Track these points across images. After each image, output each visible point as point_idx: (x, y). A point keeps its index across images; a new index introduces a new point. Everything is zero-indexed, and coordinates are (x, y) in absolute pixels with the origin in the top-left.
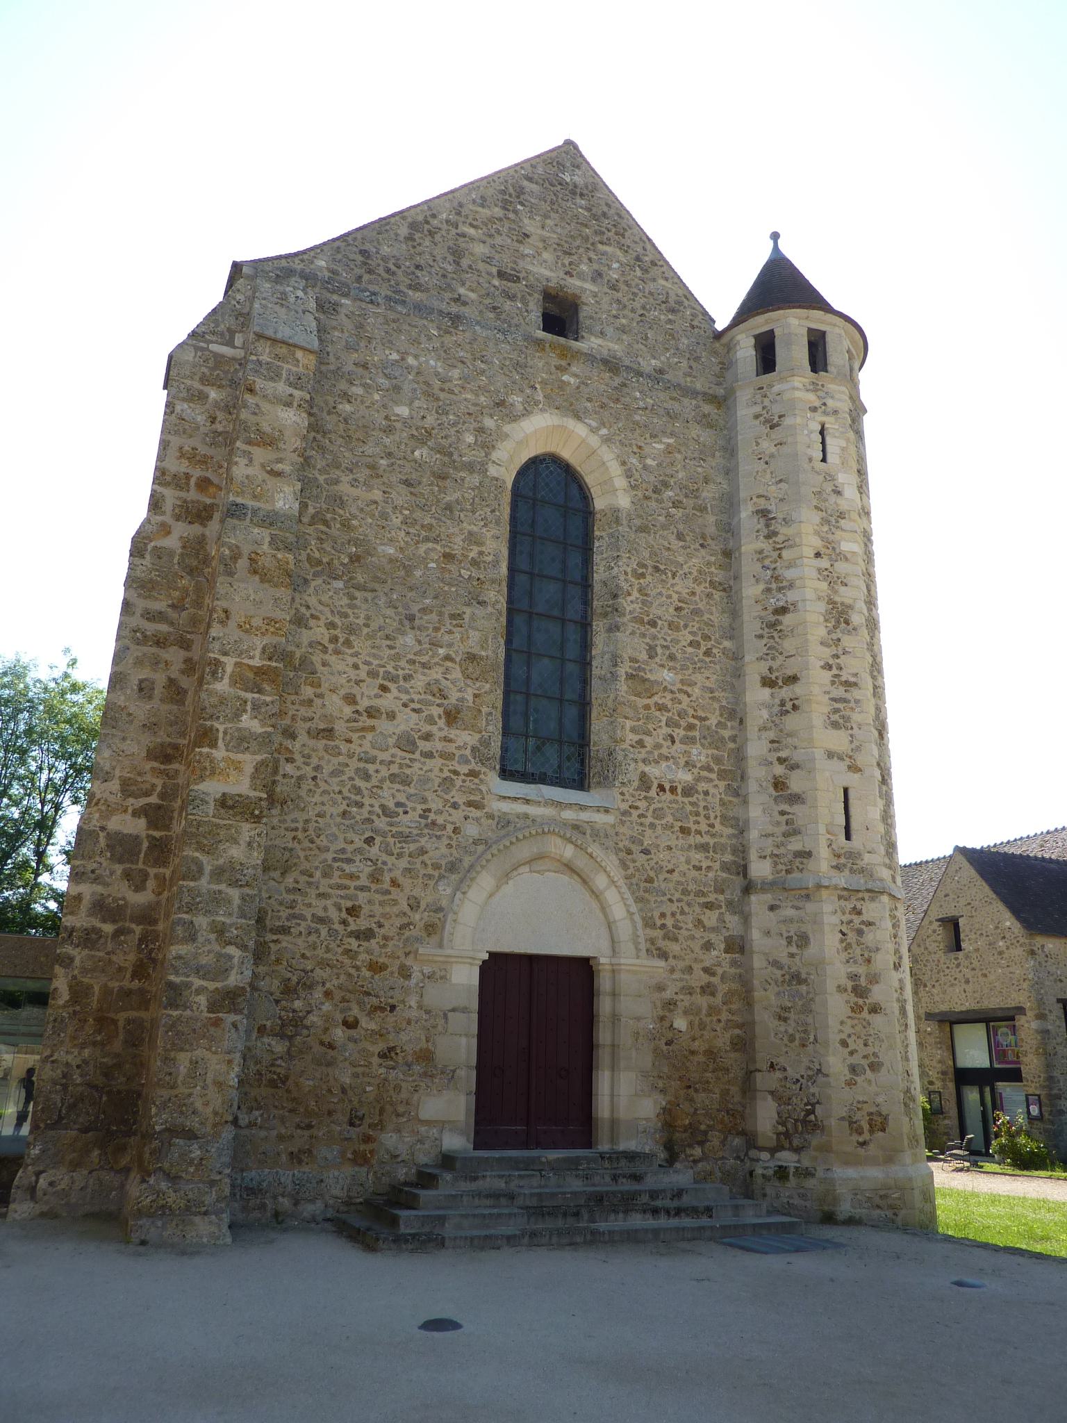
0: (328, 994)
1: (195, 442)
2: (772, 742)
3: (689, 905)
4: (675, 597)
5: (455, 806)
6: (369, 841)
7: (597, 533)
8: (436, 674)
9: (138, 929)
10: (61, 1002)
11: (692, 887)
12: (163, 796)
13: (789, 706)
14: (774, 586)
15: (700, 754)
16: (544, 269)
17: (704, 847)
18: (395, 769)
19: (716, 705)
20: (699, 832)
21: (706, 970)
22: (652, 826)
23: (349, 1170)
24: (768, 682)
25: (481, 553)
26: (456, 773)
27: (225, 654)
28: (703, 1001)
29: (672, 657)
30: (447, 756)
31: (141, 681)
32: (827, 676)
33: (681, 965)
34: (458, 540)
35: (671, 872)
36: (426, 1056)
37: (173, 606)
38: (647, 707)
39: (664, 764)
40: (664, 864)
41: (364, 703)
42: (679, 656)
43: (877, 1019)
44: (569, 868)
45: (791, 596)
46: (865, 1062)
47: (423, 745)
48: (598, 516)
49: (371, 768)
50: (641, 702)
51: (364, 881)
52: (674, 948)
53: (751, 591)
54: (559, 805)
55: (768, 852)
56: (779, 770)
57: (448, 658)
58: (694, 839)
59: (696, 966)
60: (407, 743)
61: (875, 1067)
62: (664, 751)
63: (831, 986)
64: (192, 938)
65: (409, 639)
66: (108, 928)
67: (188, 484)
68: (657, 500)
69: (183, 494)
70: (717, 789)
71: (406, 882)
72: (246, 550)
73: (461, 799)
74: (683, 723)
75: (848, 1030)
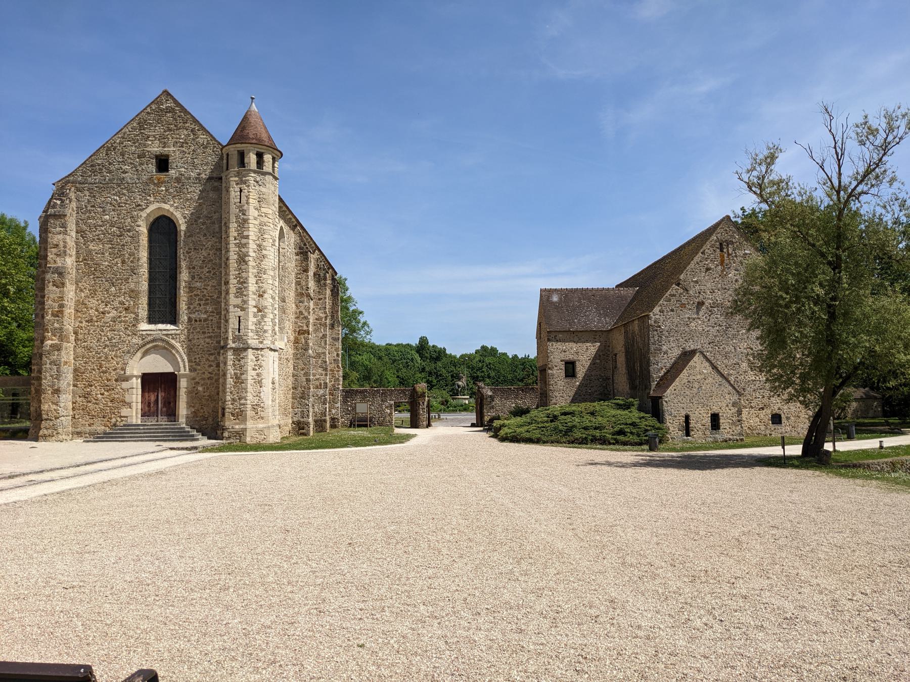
8: (122, 298)
15: (209, 308)
16: (155, 148)
17: (210, 337)
28: (209, 382)
29: (200, 278)
32: (235, 281)
34: (127, 255)
60: (114, 320)
63: (229, 376)
65: (113, 289)
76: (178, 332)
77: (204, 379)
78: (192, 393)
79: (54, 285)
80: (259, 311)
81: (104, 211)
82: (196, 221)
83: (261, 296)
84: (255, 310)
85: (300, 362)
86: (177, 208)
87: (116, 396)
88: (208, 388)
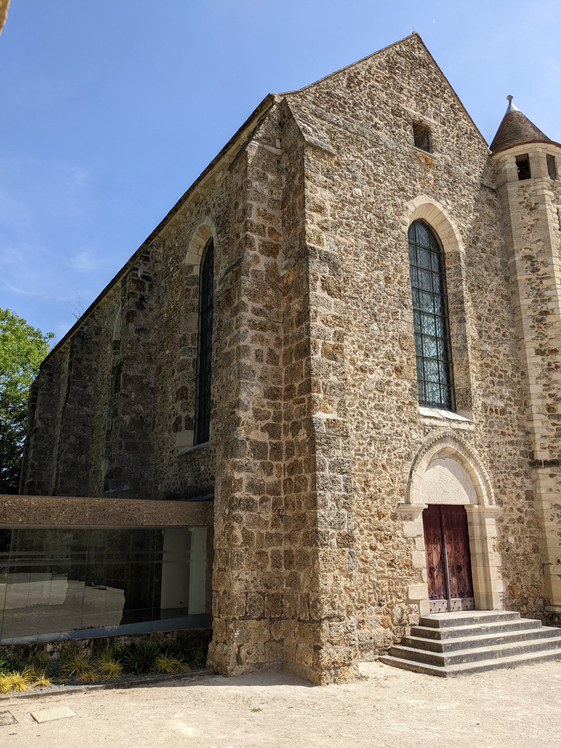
0: (361, 531)
1: (265, 205)
2: (544, 385)
3: (509, 474)
4: (487, 303)
5: (405, 422)
6: (370, 444)
7: (447, 266)
9: (271, 498)
10: (239, 544)
12: (275, 419)
13: (553, 366)
14: (539, 299)
15: (506, 392)
17: (511, 443)
19: (510, 364)
20: (509, 435)
23: (382, 629)
24: (539, 352)
25: (401, 277)
27: (318, 337)
29: (489, 337)
31: (256, 351)
33: (508, 507)
35: (500, 457)
37: (266, 306)
39: (491, 397)
40: (497, 452)
42: (492, 337)
44: (455, 456)
45: (550, 305)
48: (447, 256)
51: (369, 467)
53: (525, 302)
54: (449, 420)
55: (547, 445)
56: (550, 401)
57: (393, 337)
59: (515, 508)
60: (381, 387)
62: (490, 390)
64: (326, 504)
66: (257, 498)
67: (264, 232)
68: (475, 248)
69: (263, 238)
70: (514, 409)
72: (320, 276)
73: (407, 420)
76: (472, 427)
78: (504, 548)
79: (324, 288)
87: (397, 553)
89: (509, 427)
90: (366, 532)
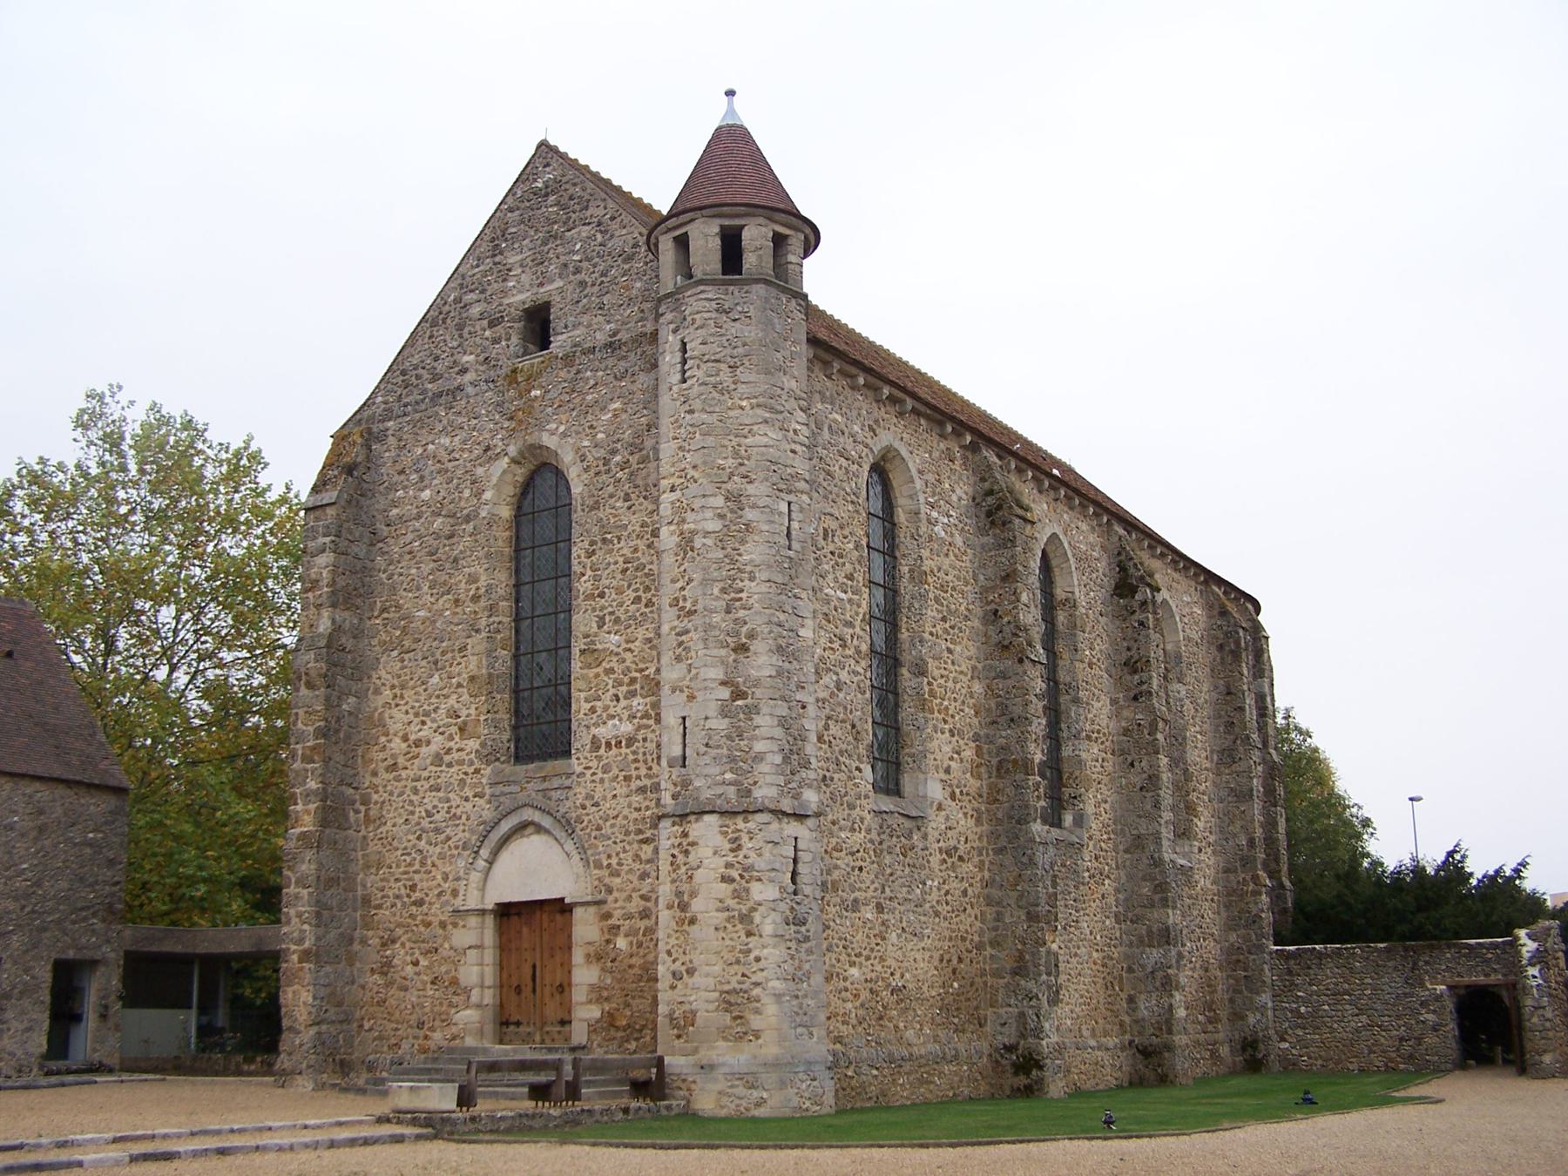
0: (403, 945)
4: (621, 560)
5: (467, 799)
6: (419, 838)
8: (452, 701)
11: (632, 828)
15: (638, 703)
16: (520, 296)
18: (432, 782)
20: (639, 777)
21: (642, 897)
22: (602, 780)
26: (466, 774)
29: (617, 621)
30: (461, 762)
33: (624, 895)
35: (615, 817)
36: (455, 982)
38: (597, 675)
39: (610, 723)
41: (413, 737)
43: (694, 929)
46: (683, 969)
47: (447, 758)
49: (418, 784)
50: (591, 673)
51: (417, 867)
52: (618, 880)
57: (459, 685)
58: (635, 784)
60: (438, 760)
61: (691, 972)
62: (612, 711)
65: (436, 679)
71: (438, 863)
73: (470, 794)
74: (626, 680)
75: (673, 941)
77: (629, 917)
80: (738, 694)
81: (422, 478)
82: (606, 462)
83: (742, 649)
84: (725, 693)
85: (1008, 860)
86: (564, 435)
88: (640, 945)
89: (641, 765)
90: (408, 945)
